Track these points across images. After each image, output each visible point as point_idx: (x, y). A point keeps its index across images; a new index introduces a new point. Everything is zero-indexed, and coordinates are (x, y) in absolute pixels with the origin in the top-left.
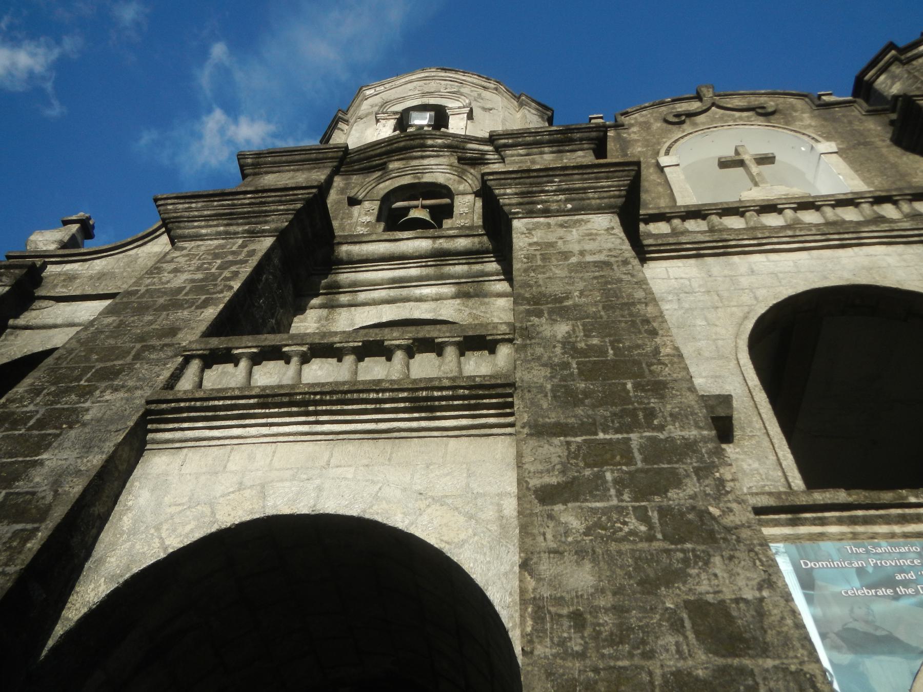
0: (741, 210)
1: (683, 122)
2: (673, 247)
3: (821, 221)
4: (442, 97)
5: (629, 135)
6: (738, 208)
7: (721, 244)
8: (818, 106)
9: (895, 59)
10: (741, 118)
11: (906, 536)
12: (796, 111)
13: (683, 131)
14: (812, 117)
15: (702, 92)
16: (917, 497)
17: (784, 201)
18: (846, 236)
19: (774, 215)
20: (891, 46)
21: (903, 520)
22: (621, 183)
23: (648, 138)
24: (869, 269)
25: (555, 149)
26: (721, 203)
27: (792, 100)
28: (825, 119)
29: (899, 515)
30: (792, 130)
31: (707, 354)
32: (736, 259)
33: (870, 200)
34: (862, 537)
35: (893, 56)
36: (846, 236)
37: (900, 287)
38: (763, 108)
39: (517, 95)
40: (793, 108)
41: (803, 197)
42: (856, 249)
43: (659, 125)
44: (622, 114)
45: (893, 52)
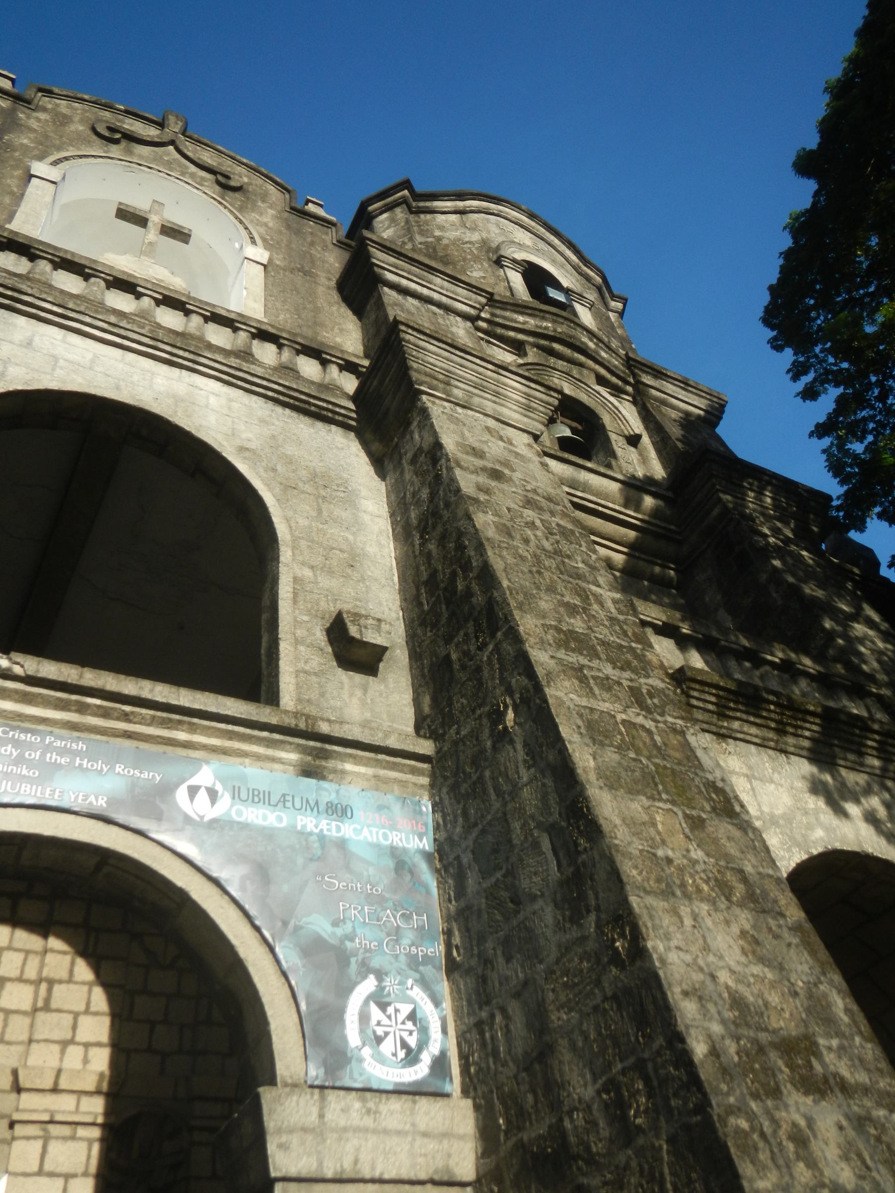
0: (87, 270)
1: (116, 142)
3: (179, 328)
5: (28, 117)
6: (85, 266)
7: (9, 293)
8: (292, 208)
9: (404, 201)
10: (193, 176)
12: (264, 201)
13: (106, 152)
14: (274, 217)
15: (168, 119)
17: (149, 286)
18: (181, 353)
19: (130, 297)
20: (406, 184)
23: (52, 134)
24: (178, 399)
26: (66, 251)
27: (271, 188)
28: (288, 227)
30: (237, 218)
32: (22, 320)
33: (253, 330)
35: (404, 197)
36: (181, 353)
37: (194, 432)
38: (228, 177)
40: (264, 197)
41: (176, 292)
42: (184, 372)
43: (81, 128)
45: (406, 192)
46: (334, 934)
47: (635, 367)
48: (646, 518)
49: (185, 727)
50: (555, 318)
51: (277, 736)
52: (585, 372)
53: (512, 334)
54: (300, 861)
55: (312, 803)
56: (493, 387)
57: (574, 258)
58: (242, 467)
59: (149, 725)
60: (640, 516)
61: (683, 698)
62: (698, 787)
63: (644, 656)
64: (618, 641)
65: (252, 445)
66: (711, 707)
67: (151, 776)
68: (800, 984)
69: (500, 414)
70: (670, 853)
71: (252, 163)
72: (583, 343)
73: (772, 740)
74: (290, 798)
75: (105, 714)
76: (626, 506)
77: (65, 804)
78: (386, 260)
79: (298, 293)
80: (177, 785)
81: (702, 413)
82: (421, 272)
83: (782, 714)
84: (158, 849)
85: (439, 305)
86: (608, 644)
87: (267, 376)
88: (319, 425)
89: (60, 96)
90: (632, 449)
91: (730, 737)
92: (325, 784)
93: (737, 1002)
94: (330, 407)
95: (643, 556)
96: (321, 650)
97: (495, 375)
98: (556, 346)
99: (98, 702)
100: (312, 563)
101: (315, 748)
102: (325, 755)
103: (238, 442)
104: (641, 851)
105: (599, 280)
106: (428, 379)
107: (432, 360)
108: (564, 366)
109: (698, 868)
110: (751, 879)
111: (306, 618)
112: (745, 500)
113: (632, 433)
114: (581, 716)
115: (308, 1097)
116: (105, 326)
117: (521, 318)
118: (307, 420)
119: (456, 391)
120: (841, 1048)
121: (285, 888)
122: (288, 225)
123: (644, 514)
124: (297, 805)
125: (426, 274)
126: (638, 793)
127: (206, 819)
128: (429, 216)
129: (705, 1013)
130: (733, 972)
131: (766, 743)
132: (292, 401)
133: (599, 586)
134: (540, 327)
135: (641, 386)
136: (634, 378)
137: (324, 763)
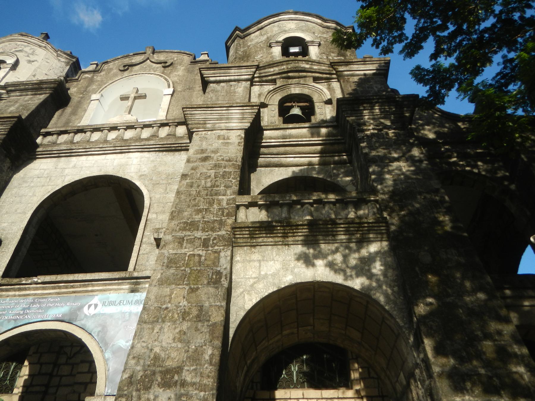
2: (48, 152)
4: (8, 55)
11: (20, 296)
16: (26, 281)
17: (122, 125)
18: (124, 148)
20: (237, 29)
21: (20, 290)
22: (7, 127)
24: (121, 166)
25: (33, 93)
29: (18, 288)
31: (19, 211)
32: (74, 159)
33: (159, 125)
34: (4, 296)
35: (236, 35)
36: (124, 148)
38: (166, 63)
39: (57, 50)
44: (104, 63)
45: (237, 32)
46: (126, 345)
47: (335, 65)
48: (324, 138)
49: (91, 285)
50: (287, 62)
51: (120, 281)
52: (308, 79)
53: (270, 78)
54: (120, 322)
55: (130, 302)
56: (226, 116)
57: (319, 21)
58: (138, 183)
59: (80, 288)
60: (321, 139)
61: (232, 236)
62: (209, 275)
64: (215, 218)
65: (145, 173)
66: (246, 236)
67: (78, 304)
68: (194, 347)
69: (228, 127)
70: (169, 305)
71: (179, 51)
72: (302, 67)
73: (280, 241)
74: (122, 302)
75: (66, 287)
76: (312, 137)
77: (49, 319)
78: (209, 73)
79: (184, 99)
80: (85, 305)
81: (374, 71)
82: (225, 71)
83: (284, 230)
84: (76, 327)
85: (235, 81)
86: (208, 222)
87: (155, 144)
88: (177, 153)
89: (110, 62)
90: (329, 106)
91: (258, 245)
92: (137, 294)
93: (156, 358)
94: (180, 145)
95: (328, 155)
96: (152, 244)
97: (227, 111)
98: (290, 74)
99: (63, 284)
100: (157, 211)
101: (134, 282)
102: (139, 284)
103: (140, 173)
104: (155, 307)
105: (334, 25)
106: (196, 126)
107: (197, 117)
108: (296, 81)
109: (179, 309)
110: (204, 308)
111: (149, 234)
112: (362, 116)
113: (327, 99)
114: (168, 258)
115: (100, 399)
116: (98, 149)
117: (272, 70)
118: (172, 153)
119: (208, 126)
120: (195, 370)
121: (112, 333)
122: (188, 71)
123: (323, 137)
124: (124, 304)
125: (227, 71)
126: (173, 284)
127: (91, 315)
128: (248, 37)
129: (137, 364)
130: (162, 347)
131: (277, 244)
132: (165, 149)
133: (224, 195)
134: (281, 70)
135: (338, 73)
136: (335, 70)
137: (138, 286)
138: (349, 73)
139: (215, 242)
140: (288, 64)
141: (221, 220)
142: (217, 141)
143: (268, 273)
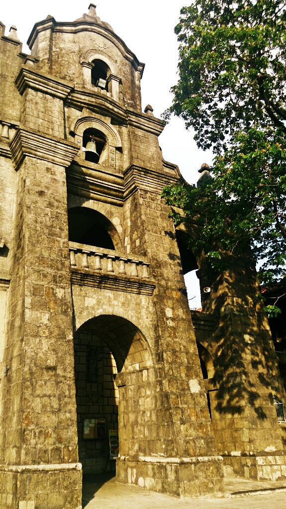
20: (52, 19)
47: (129, 113)
53: (79, 104)
56: (53, 150)
57: (123, 49)
63: (64, 263)
69: (54, 160)
105: (132, 58)
117: (83, 97)
133: (60, 237)
134: (90, 101)
138: (137, 124)
139: (60, 279)
140: (97, 98)
141: (61, 260)
142: (47, 175)
143: (89, 306)
